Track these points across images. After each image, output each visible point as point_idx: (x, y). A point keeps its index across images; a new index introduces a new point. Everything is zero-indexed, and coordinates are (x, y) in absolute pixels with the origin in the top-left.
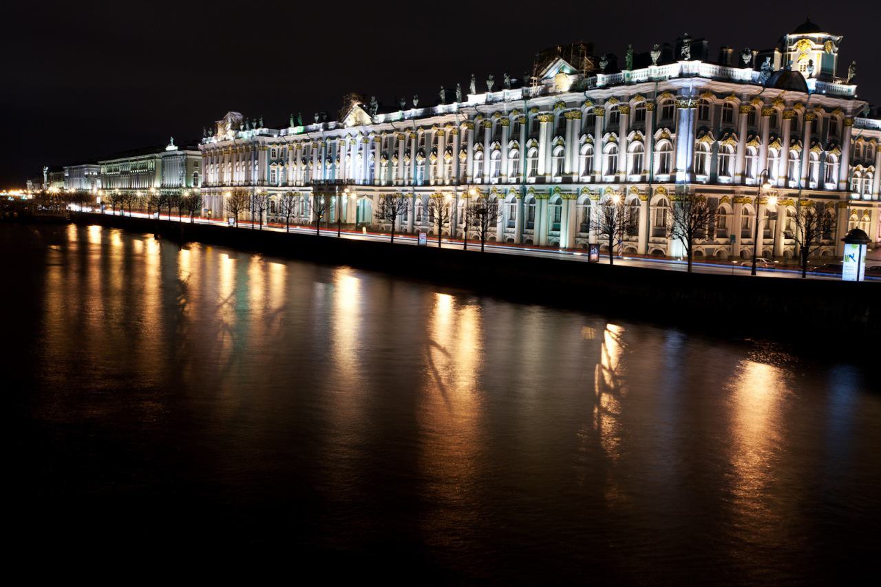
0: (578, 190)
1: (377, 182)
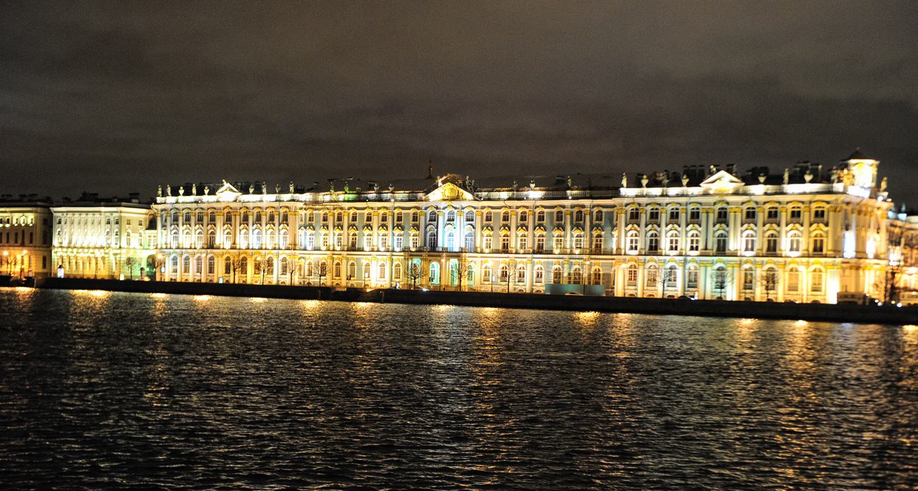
0: (741, 261)
1: (479, 250)
